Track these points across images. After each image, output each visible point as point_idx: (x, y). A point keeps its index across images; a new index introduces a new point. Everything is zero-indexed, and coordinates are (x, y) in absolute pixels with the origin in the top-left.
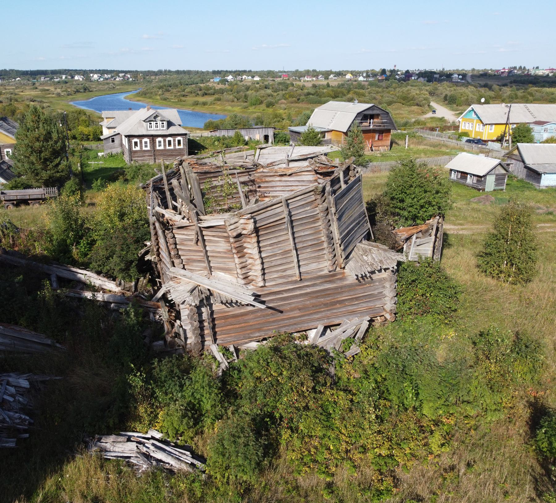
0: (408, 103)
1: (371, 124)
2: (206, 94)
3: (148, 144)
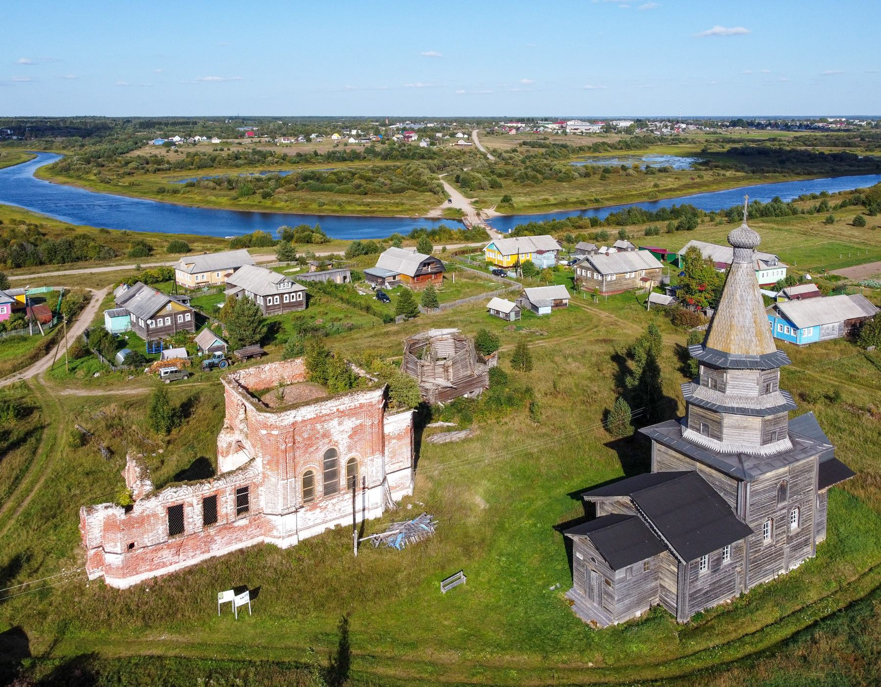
2: (159, 170)
3: (278, 300)
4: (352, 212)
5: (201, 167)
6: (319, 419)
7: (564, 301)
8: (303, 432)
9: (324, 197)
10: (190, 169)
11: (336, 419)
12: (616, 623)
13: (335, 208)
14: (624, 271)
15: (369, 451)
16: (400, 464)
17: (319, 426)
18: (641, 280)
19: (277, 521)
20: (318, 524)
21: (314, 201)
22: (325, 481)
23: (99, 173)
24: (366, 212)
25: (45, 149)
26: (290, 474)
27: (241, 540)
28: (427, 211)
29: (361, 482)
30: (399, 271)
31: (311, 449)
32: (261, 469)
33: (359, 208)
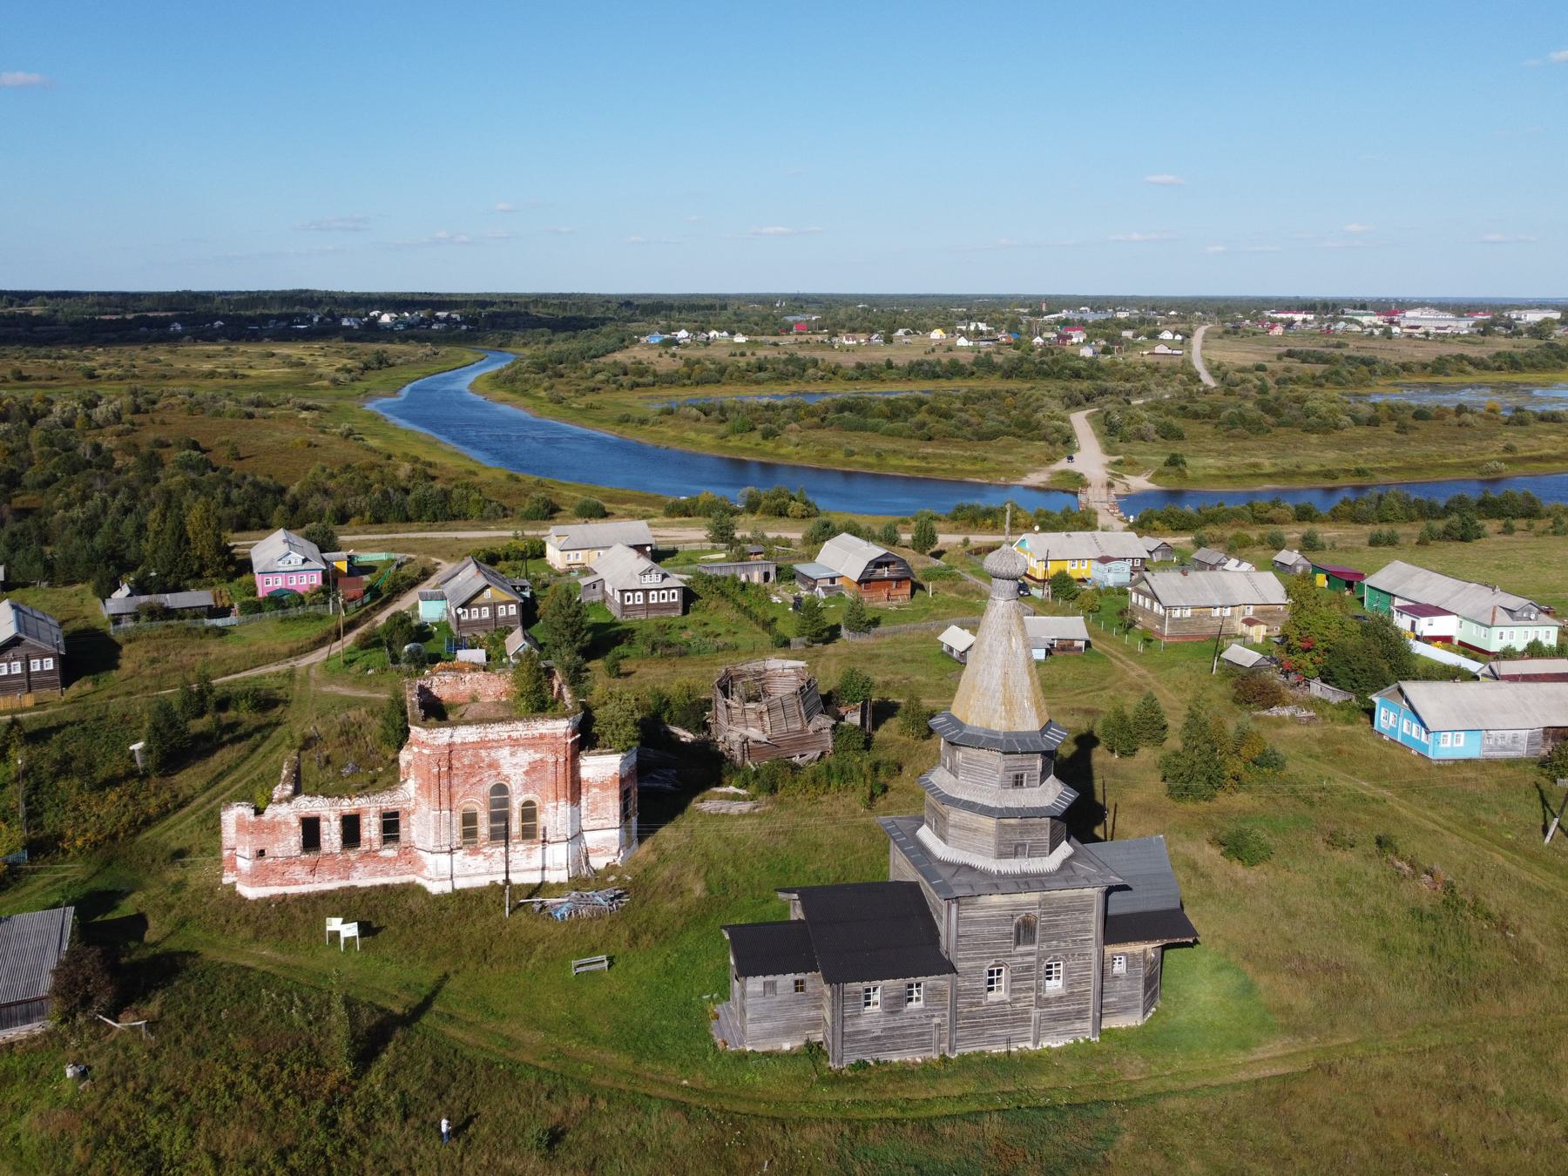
0: (1029, 435)
1: (885, 572)
2: (638, 385)
4: (896, 468)
5: (701, 382)
6: (483, 744)
7: (1077, 644)
8: (463, 757)
9: (857, 441)
10: (684, 385)
12: (749, 1049)
13: (872, 460)
14: (1207, 604)
15: (551, 795)
17: (483, 753)
18: (1244, 621)
19: (429, 859)
20: (480, 874)
21: (840, 446)
22: (492, 822)
23: (552, 387)
24: (919, 469)
25: (500, 346)
26: (445, 805)
27: (387, 874)
28: (1023, 474)
30: (841, 572)
31: (474, 780)
32: (413, 794)
33: (909, 463)
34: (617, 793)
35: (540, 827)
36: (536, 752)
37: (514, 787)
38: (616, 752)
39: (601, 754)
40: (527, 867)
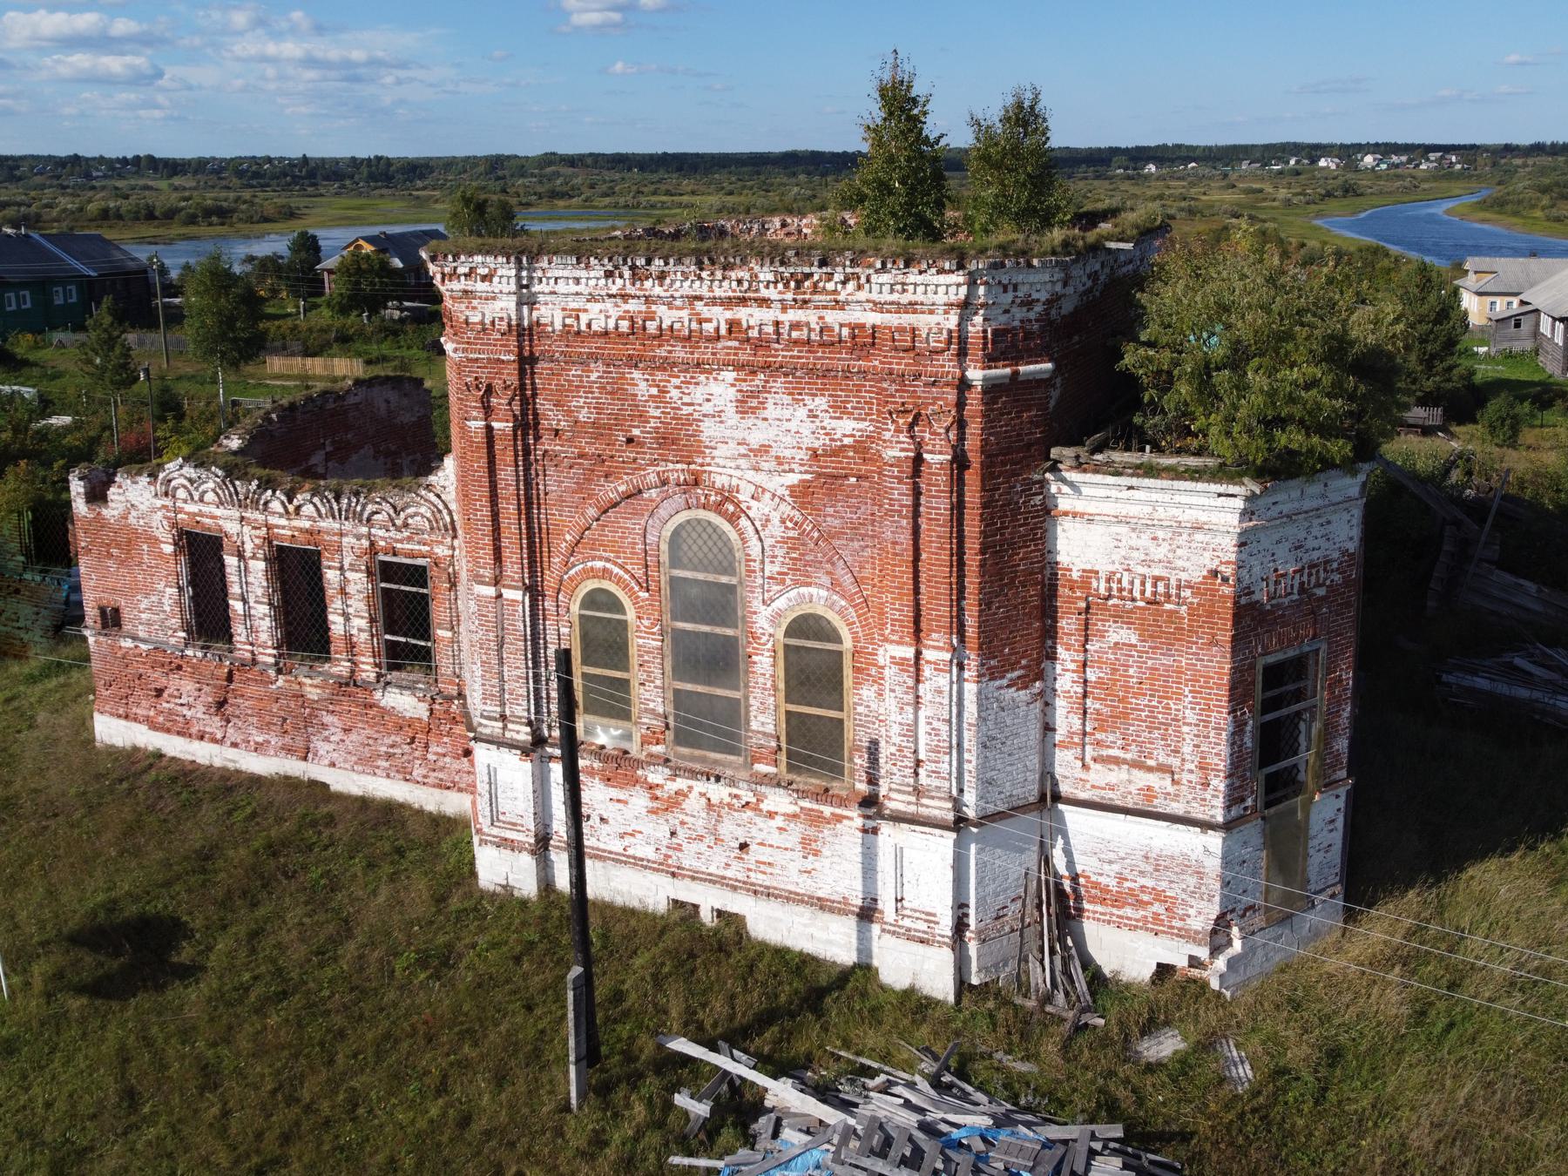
11: (729, 375)
15: (898, 610)
16: (1154, 780)
20: (638, 863)
26: (513, 568)
29: (861, 761)
34: (1217, 664)
35: (856, 736)
36: (839, 409)
37: (755, 549)
38: (1219, 474)
39: (1150, 471)
40: (805, 886)
